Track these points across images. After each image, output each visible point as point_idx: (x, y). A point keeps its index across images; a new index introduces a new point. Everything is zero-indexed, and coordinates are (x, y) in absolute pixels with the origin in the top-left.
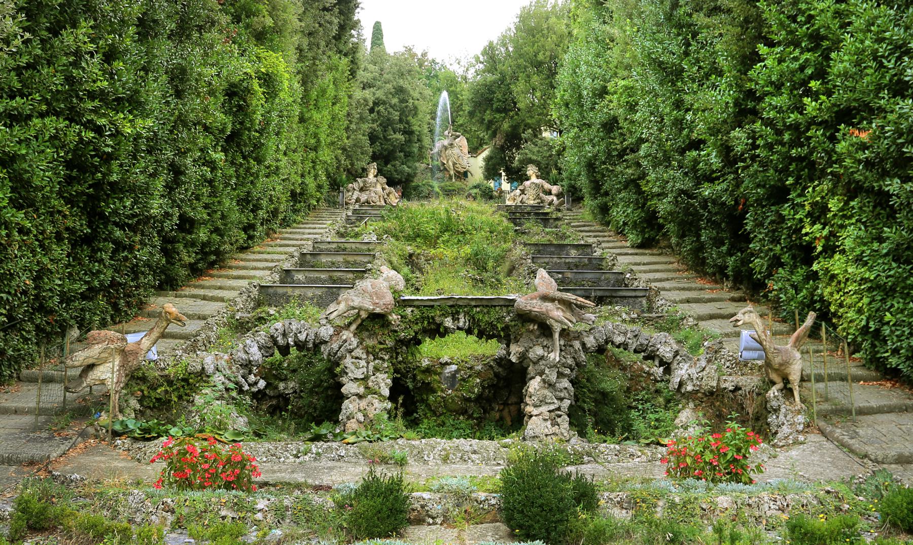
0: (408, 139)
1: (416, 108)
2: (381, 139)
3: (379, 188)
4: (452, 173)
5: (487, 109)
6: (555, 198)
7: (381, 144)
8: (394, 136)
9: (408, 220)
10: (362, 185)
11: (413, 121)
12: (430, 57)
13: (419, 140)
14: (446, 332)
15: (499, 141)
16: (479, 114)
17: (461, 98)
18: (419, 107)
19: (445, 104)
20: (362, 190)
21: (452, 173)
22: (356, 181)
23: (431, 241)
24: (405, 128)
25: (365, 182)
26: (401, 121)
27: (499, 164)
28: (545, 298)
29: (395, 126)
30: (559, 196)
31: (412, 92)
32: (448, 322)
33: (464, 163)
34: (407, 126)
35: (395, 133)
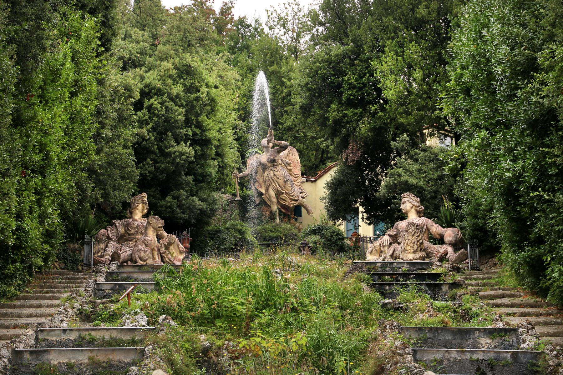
0: (199, 153)
1: (212, 101)
2: (153, 153)
3: (151, 236)
4: (275, 208)
5: (331, 102)
6: (450, 250)
7: (155, 162)
8: (177, 148)
10: (122, 230)
11: (208, 122)
12: (236, 14)
13: (218, 155)
16: (318, 110)
17: (289, 83)
18: (218, 99)
19: (262, 93)
20: (122, 239)
21: (275, 208)
22: (112, 224)
24: (195, 134)
25: (127, 225)
26: (188, 123)
27: (353, 194)
29: (178, 131)
30: (457, 245)
31: (206, 75)
33: (295, 192)
34: (198, 131)
35: (178, 144)
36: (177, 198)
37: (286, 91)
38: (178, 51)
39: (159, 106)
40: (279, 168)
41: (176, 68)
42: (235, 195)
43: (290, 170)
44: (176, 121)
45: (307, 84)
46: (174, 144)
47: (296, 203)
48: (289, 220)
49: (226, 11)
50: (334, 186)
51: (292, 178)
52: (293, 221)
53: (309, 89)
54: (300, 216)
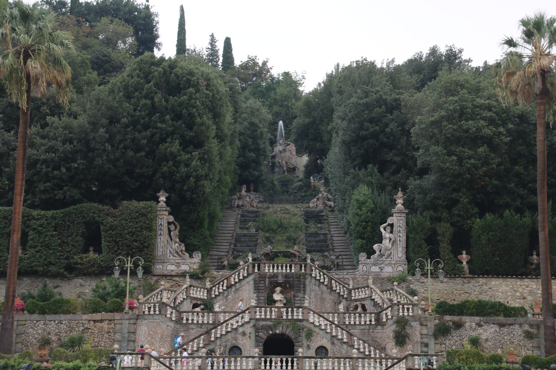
1: (262, 133)
4: (285, 168)
8: (249, 154)
10: (239, 196)
14: (279, 256)
17: (292, 111)
19: (281, 127)
20: (239, 198)
23: (275, 231)
24: (255, 147)
25: (240, 195)
28: (295, 251)
32: (279, 255)
33: (293, 162)
34: (256, 146)
35: (250, 152)
42: (269, 162)
49: (264, 63)
51: (292, 156)
54: (295, 170)
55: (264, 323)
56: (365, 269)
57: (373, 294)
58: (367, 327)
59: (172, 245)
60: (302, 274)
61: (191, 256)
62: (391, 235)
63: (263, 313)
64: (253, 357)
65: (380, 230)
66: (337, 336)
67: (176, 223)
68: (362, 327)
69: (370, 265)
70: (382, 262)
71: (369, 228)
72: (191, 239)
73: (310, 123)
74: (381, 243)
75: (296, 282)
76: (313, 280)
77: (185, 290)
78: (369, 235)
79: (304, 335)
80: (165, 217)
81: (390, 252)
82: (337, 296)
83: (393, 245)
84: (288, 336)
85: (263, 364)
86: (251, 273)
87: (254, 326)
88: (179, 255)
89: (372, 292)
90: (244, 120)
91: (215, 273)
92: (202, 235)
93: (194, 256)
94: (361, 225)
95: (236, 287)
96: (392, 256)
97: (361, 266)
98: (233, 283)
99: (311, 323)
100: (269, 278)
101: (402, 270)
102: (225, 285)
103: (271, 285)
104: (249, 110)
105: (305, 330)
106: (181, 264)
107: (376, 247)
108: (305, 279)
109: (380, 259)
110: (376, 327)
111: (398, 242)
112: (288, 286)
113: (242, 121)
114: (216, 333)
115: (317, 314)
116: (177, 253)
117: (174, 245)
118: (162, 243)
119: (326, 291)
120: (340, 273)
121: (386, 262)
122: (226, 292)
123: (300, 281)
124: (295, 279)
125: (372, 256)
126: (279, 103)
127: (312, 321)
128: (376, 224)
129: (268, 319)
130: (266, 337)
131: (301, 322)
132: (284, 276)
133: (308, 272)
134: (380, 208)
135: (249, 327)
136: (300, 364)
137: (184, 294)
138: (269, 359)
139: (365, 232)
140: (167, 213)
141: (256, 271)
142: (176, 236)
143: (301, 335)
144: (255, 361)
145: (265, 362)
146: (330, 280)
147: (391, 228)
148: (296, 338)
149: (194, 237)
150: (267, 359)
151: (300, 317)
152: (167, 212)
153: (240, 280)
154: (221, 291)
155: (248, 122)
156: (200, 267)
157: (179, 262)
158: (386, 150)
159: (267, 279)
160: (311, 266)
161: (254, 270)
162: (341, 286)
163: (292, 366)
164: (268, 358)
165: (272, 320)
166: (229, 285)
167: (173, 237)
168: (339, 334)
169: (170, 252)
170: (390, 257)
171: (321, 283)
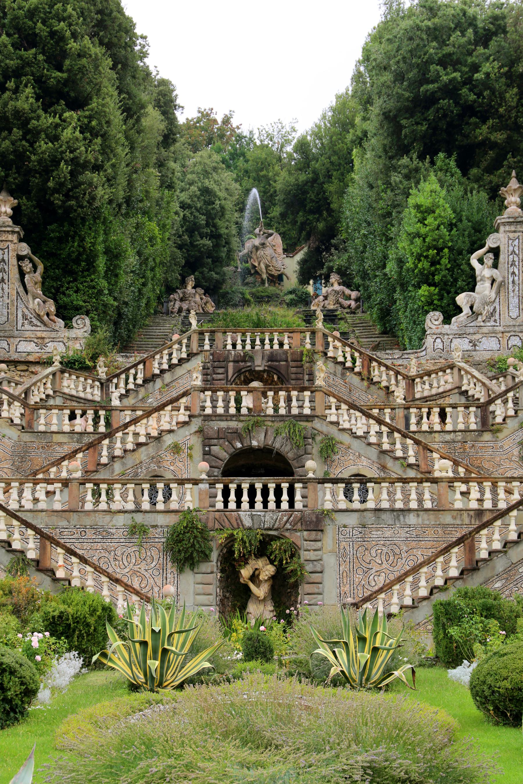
1: (222, 208)
3: (198, 298)
4: (265, 276)
5: (299, 211)
7: (188, 251)
8: (201, 242)
9: (231, 321)
10: (181, 295)
11: (220, 223)
15: (313, 243)
16: (291, 216)
17: (274, 184)
20: (182, 300)
21: (265, 276)
22: (176, 292)
24: (212, 231)
25: (184, 293)
26: (207, 225)
29: (202, 230)
33: (279, 265)
34: (213, 229)
36: (202, 273)
37: (272, 190)
38: (200, 177)
39: (190, 215)
40: (268, 248)
41: (200, 190)
43: (275, 250)
44: (200, 224)
45: (284, 200)
46: (199, 239)
47: (280, 273)
48: (275, 284)
50: (303, 263)
51: (277, 255)
52: (277, 285)
53: (285, 203)
54: (282, 280)
55: (223, 424)
56: (440, 346)
57: (465, 381)
58: (459, 437)
59: (28, 301)
60: (305, 352)
61: (68, 326)
62: (495, 270)
63: (220, 403)
64: (196, 482)
65: (470, 265)
66: (392, 451)
67: (36, 259)
68: (448, 437)
69: (451, 337)
70: (477, 328)
71: (444, 261)
72: (69, 296)
73: (306, 183)
74: (473, 290)
75: (294, 370)
76: (331, 365)
77: (51, 377)
78: (444, 276)
79: (315, 450)
80: (12, 246)
81: (492, 308)
82: (382, 393)
83: (498, 293)
84: (278, 454)
85: (220, 497)
86: (195, 351)
87: (200, 431)
88: (42, 322)
89: (461, 377)
90: (191, 184)
91: (121, 359)
92: (94, 287)
93: (75, 325)
94: (426, 257)
95: (163, 381)
96: (497, 317)
97: (429, 341)
98: (157, 372)
99: (332, 423)
100: (234, 361)
101: (520, 344)
102: (140, 376)
103: (239, 377)
104: (198, 168)
105: (319, 438)
106: (47, 340)
107: (462, 299)
108: (312, 362)
109: (472, 324)
110: (481, 435)
111: (511, 286)
112: (275, 377)
113: (188, 186)
114: (110, 448)
115: (346, 402)
116: (39, 317)
117: (31, 302)
118: (5, 298)
119: (359, 386)
120: (387, 356)
121: (485, 330)
122: (142, 389)
123: (302, 366)
124: (292, 364)
125: (454, 319)
126: (253, 174)
127: (334, 418)
128: (460, 253)
129: (233, 416)
130: (227, 457)
131: (307, 421)
132: (266, 358)
133: (319, 347)
134: (469, 221)
135: (187, 433)
136: (311, 495)
137: (49, 385)
138: (235, 486)
139: (436, 270)
140: (15, 238)
141: (207, 347)
142: (36, 283)
143: (309, 451)
144: (200, 490)
145: (226, 493)
146: (366, 363)
147: (494, 256)
148: (299, 457)
149: (76, 292)
150: (230, 486)
151: (307, 411)
152: (16, 235)
153: (172, 366)
154: (131, 386)
155: (198, 187)
156: (89, 345)
157: (43, 336)
158: (473, 120)
159: (231, 365)
160: (325, 336)
161: (201, 345)
162: (391, 373)
163: (291, 503)
164: (232, 482)
165: (242, 418)
166: (149, 375)
167: (29, 286)
168: (398, 446)
169: (25, 317)
170: (493, 319)
171: (348, 368)
